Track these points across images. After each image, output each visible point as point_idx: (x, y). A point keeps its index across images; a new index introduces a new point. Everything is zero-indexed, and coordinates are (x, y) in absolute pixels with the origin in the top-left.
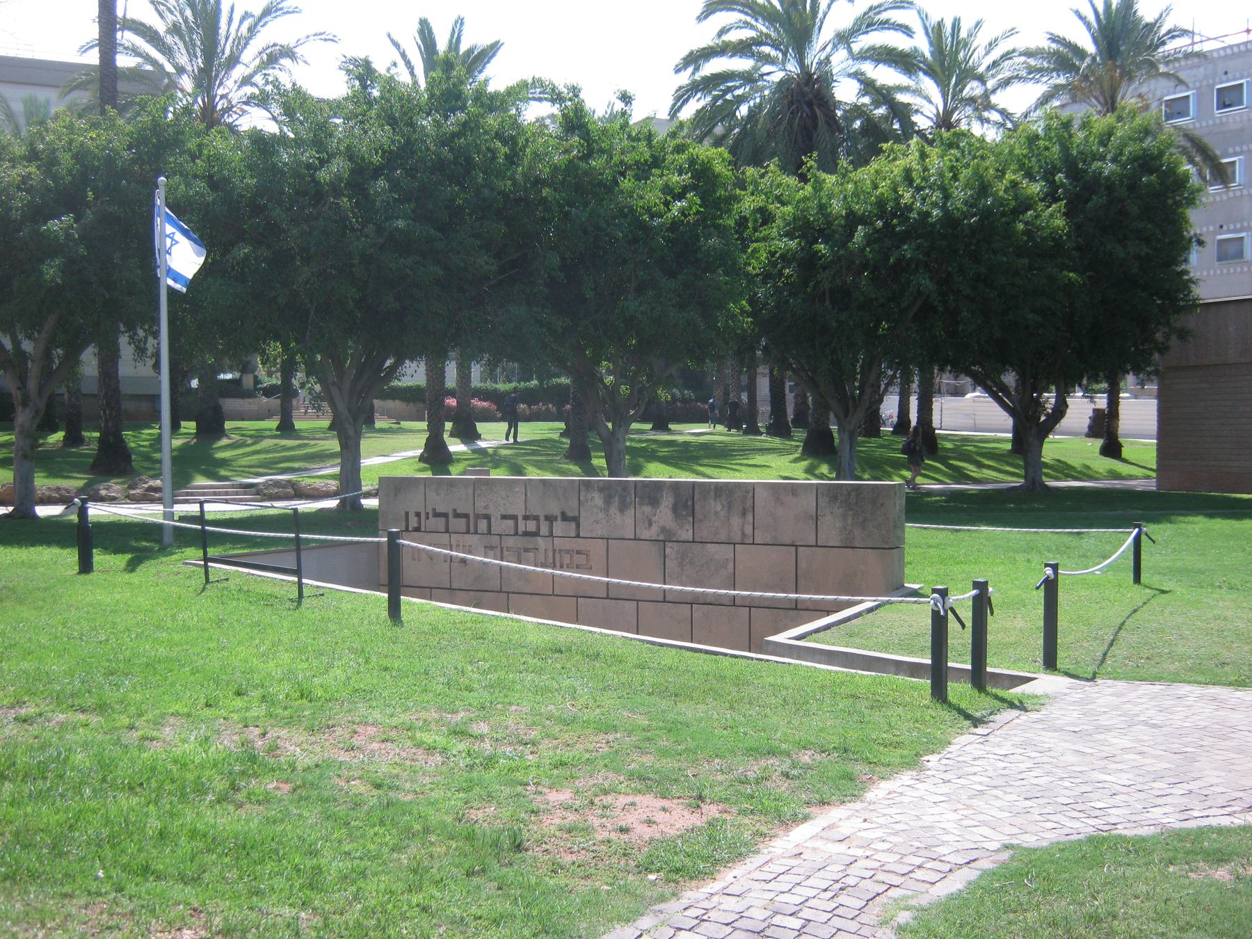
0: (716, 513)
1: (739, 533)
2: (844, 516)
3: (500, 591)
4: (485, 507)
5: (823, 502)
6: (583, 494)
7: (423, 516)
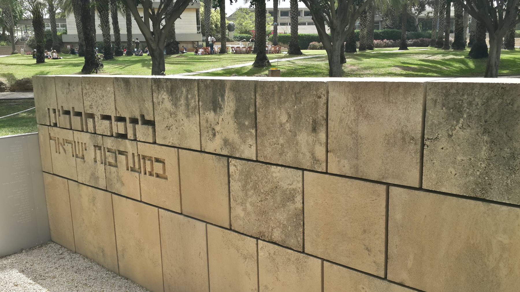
0: (281, 125)
1: (308, 155)
2: (474, 145)
3: (106, 191)
4: (91, 107)
5: (436, 114)
6: (155, 95)
7: (57, 112)
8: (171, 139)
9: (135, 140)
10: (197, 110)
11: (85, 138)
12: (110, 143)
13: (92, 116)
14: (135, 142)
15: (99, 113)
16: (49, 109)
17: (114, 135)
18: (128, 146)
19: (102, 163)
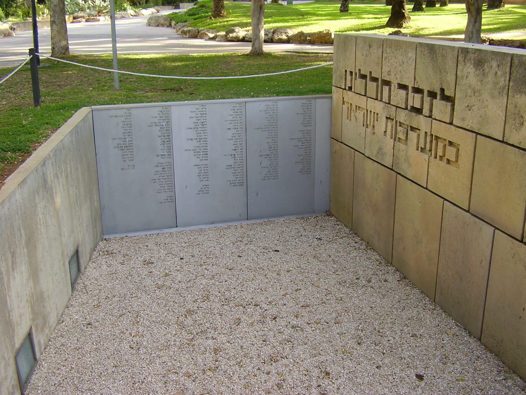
3: (392, 170)
4: (389, 73)
8: (471, 121)
9: (430, 117)
10: (505, 91)
11: (378, 107)
12: (403, 116)
13: (387, 83)
14: (430, 119)
15: (397, 81)
16: (346, 71)
17: (409, 108)
18: (421, 122)
19: (392, 138)
